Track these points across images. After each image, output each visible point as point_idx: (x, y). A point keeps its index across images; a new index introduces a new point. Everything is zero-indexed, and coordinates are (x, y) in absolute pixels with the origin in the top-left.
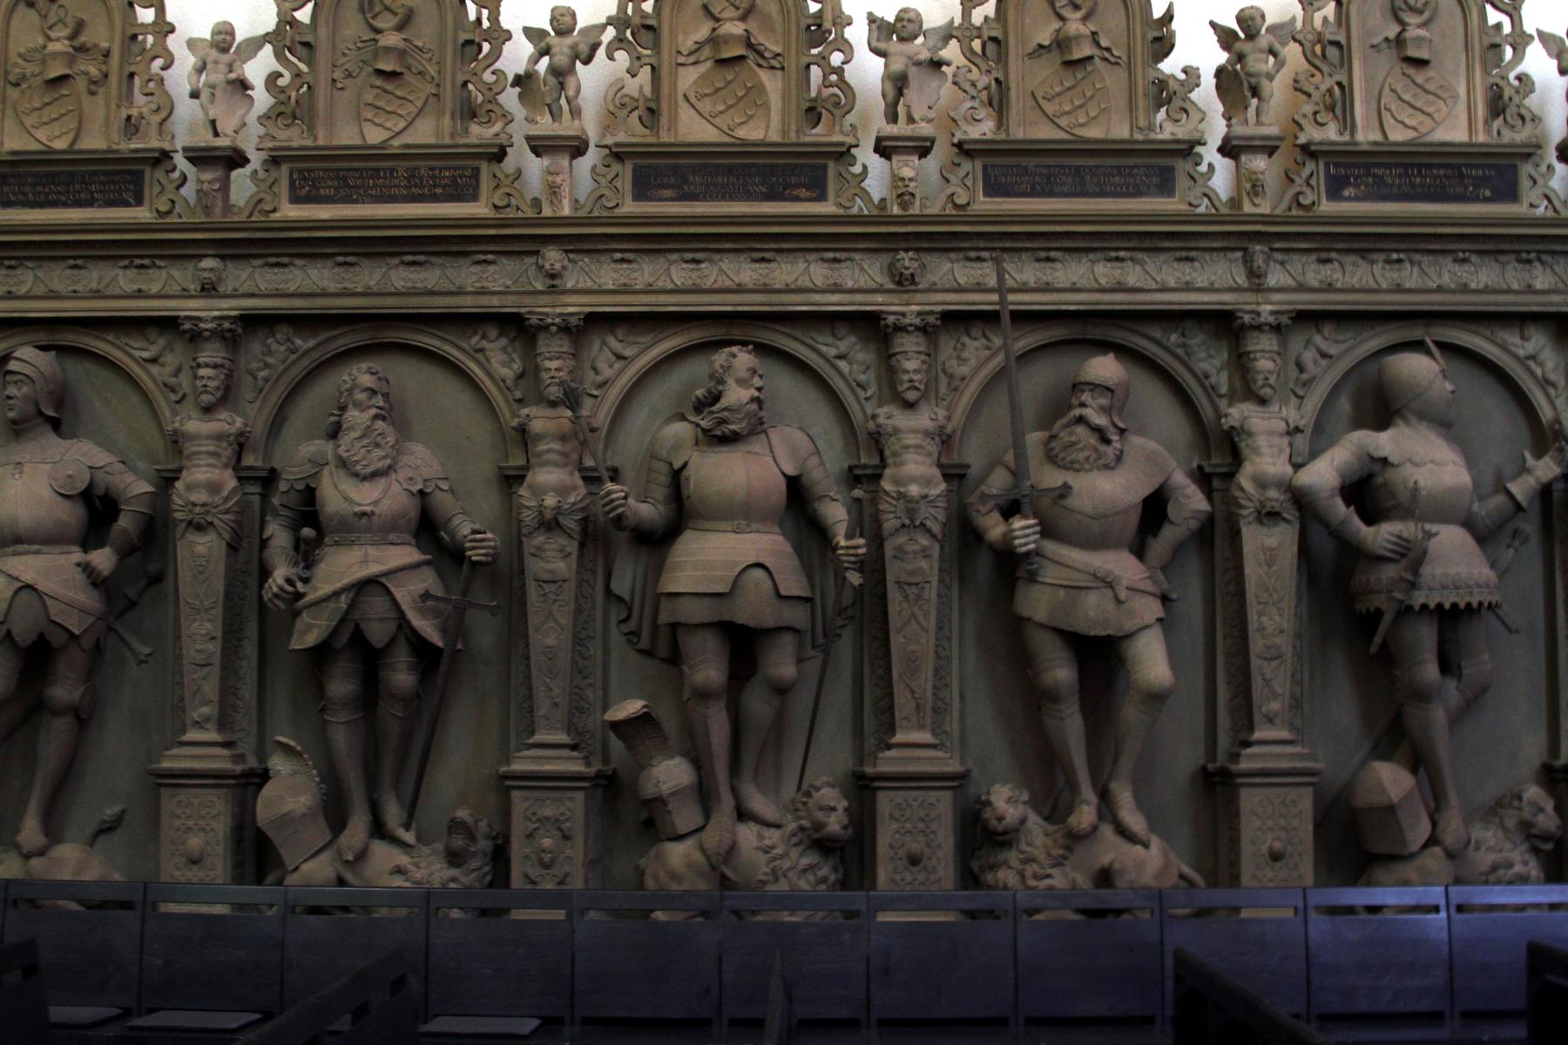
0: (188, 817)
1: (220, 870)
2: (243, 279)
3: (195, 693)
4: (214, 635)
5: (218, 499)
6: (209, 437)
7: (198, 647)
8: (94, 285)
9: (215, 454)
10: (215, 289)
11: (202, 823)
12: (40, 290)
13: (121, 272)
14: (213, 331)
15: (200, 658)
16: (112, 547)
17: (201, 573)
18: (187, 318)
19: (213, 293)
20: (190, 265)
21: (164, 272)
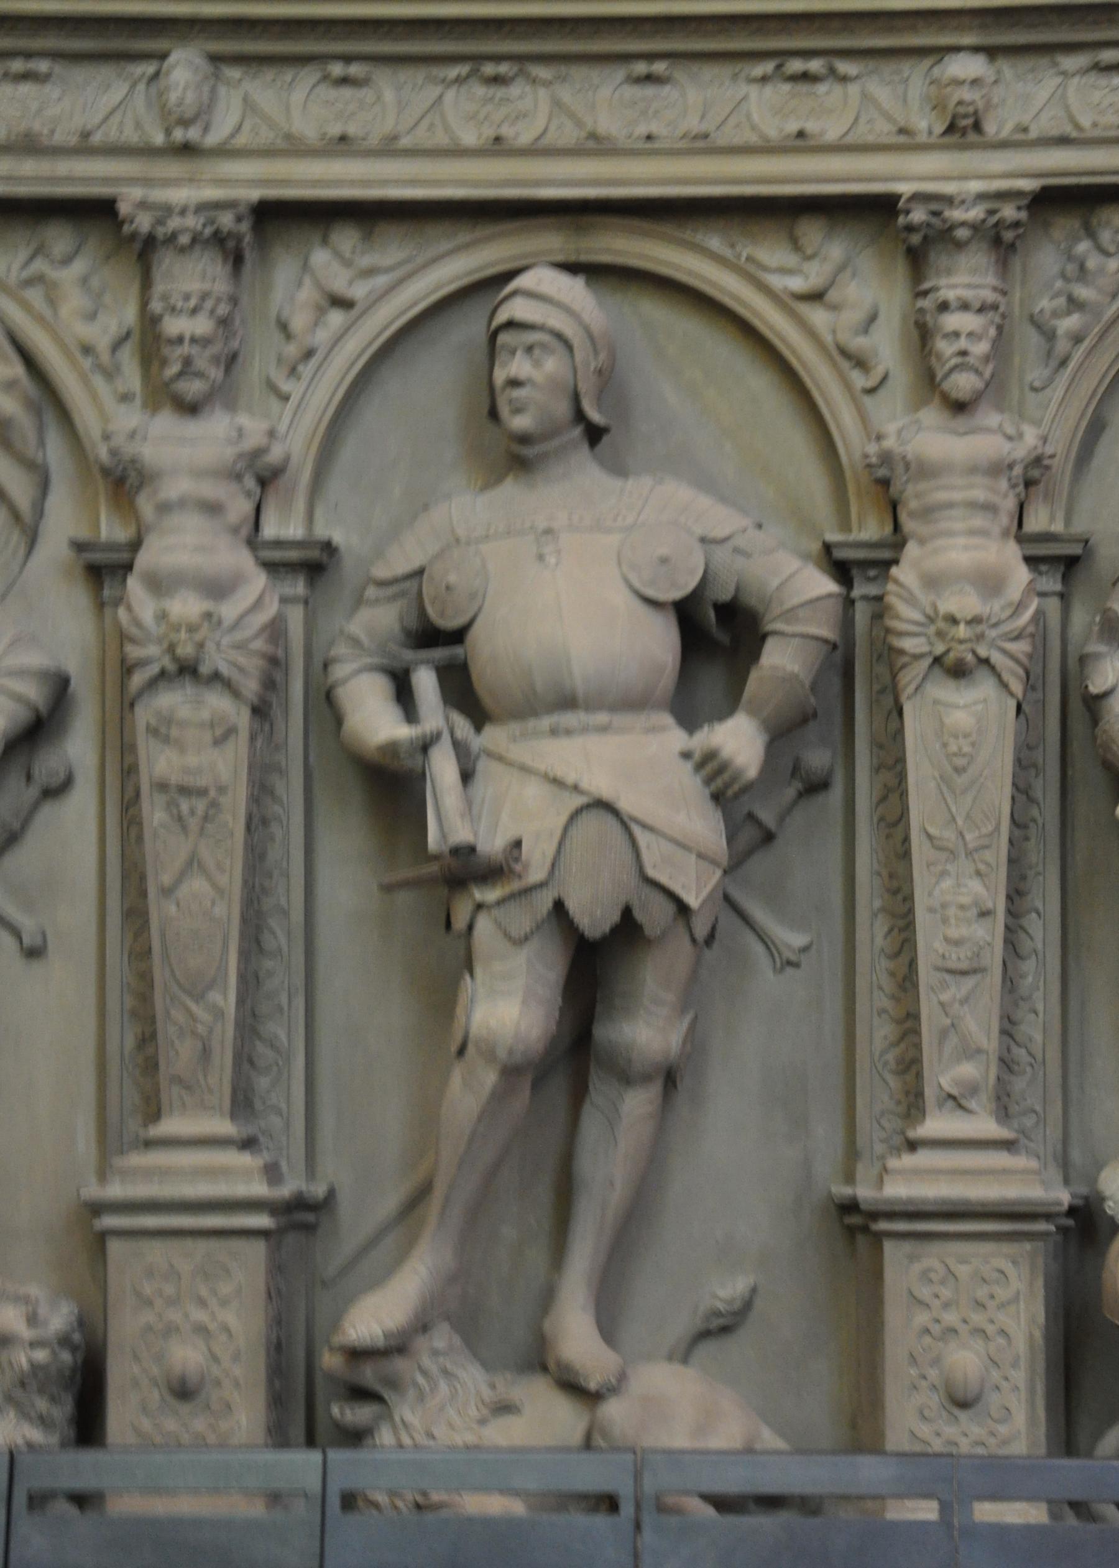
0: (946, 1306)
1: (1020, 1418)
2: (1039, 103)
3: (943, 1034)
4: (990, 905)
5: (995, 608)
6: (973, 470)
7: (954, 933)
8: (692, 124)
9: (989, 508)
10: (977, 127)
11: (978, 1318)
12: (567, 134)
13: (753, 90)
14: (975, 227)
15: (959, 958)
16: (753, 712)
17: (960, 770)
18: (917, 197)
19: (972, 137)
20: (916, 73)
21: (853, 89)
